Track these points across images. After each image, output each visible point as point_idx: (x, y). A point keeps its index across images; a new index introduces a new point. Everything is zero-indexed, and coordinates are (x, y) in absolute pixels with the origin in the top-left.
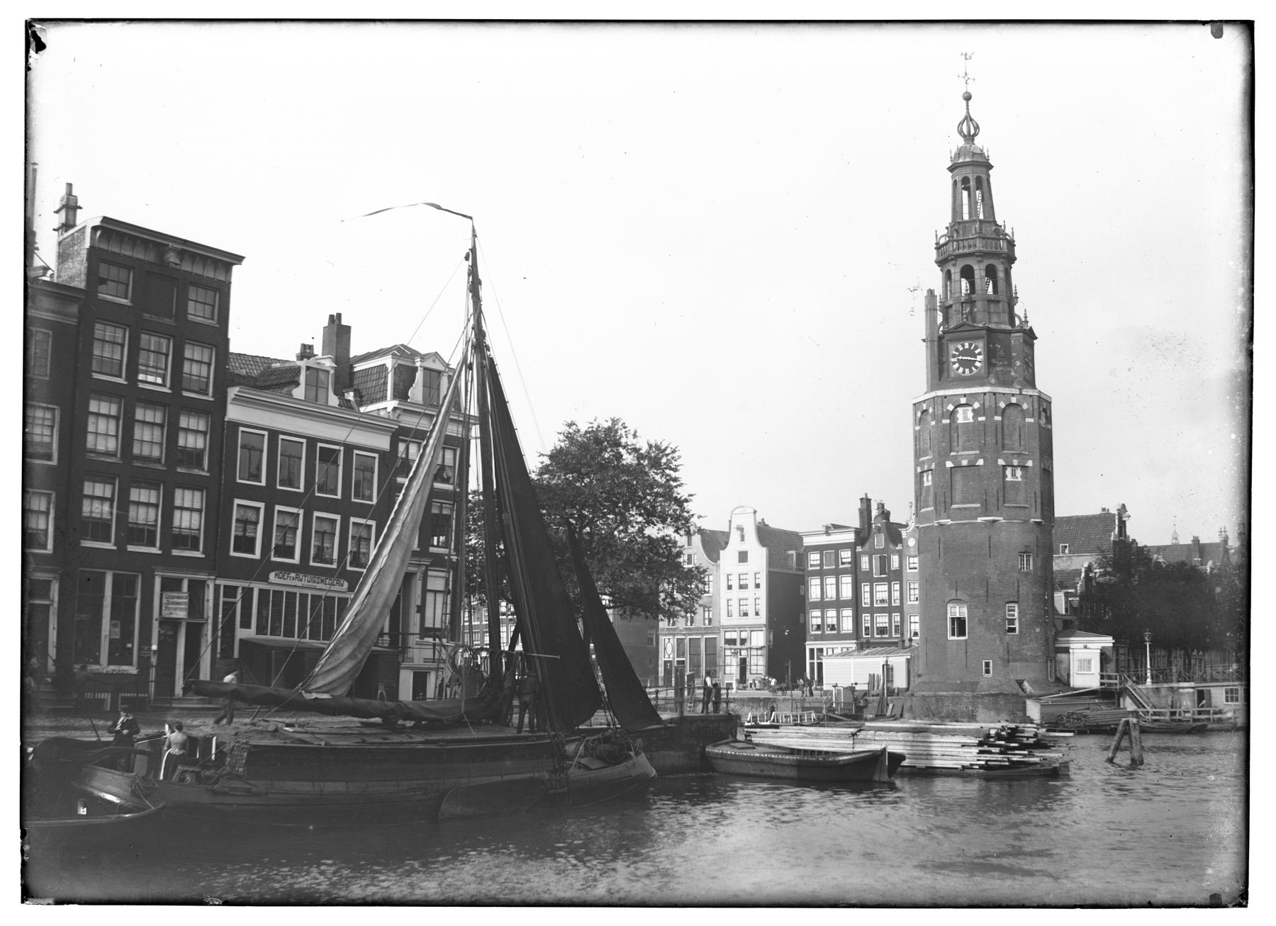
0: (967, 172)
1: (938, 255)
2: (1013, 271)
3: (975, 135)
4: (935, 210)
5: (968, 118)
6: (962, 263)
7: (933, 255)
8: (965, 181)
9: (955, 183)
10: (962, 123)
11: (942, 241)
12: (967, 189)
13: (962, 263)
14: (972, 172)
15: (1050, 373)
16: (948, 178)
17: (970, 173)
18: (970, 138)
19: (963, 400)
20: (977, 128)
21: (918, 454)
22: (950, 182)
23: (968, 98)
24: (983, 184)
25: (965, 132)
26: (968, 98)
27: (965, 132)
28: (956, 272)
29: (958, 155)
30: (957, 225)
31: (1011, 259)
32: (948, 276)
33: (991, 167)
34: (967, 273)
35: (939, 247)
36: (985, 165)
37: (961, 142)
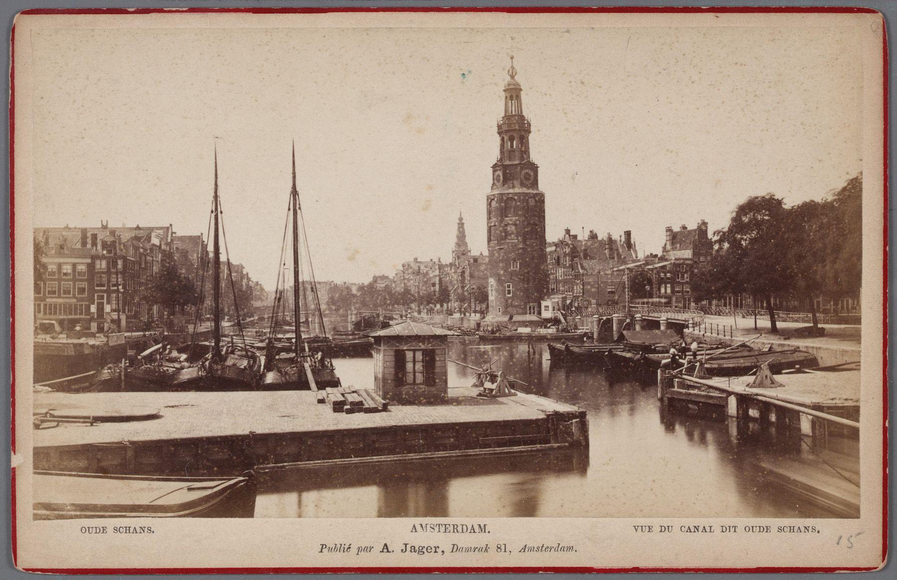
5: (513, 68)
7: (496, 129)
12: (512, 100)
14: (514, 93)
18: (512, 77)
21: (489, 218)
23: (512, 58)
24: (518, 97)
26: (512, 58)
28: (506, 138)
29: (509, 85)
30: (508, 117)
31: (530, 132)
32: (503, 139)
33: (521, 90)
34: (511, 139)
35: (499, 127)
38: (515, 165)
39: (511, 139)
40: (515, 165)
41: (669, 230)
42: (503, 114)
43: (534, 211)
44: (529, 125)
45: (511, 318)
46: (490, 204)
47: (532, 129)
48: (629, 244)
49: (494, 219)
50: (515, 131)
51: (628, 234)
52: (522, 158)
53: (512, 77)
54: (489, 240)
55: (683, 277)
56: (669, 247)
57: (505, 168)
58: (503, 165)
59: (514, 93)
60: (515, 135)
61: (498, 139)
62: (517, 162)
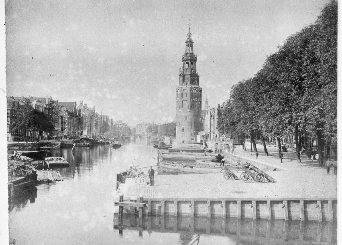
0: (189, 43)
1: (183, 59)
2: (196, 63)
3: (191, 36)
6: (186, 61)
7: (181, 59)
8: (188, 45)
10: (188, 33)
11: (183, 57)
12: (189, 46)
13: (186, 61)
16: (185, 44)
17: (189, 43)
18: (190, 36)
19: (185, 88)
20: (191, 34)
22: (185, 45)
25: (189, 35)
26: (190, 28)
27: (189, 35)
28: (185, 63)
30: (186, 54)
31: (196, 61)
32: (184, 63)
33: (193, 42)
34: (187, 63)
35: (183, 58)
44: (196, 58)
45: (183, 142)
47: (197, 59)
49: (178, 98)
52: (191, 72)
54: (177, 107)
57: (184, 76)
58: (183, 75)
59: (190, 43)
60: (189, 62)
61: (182, 63)
62: (189, 74)
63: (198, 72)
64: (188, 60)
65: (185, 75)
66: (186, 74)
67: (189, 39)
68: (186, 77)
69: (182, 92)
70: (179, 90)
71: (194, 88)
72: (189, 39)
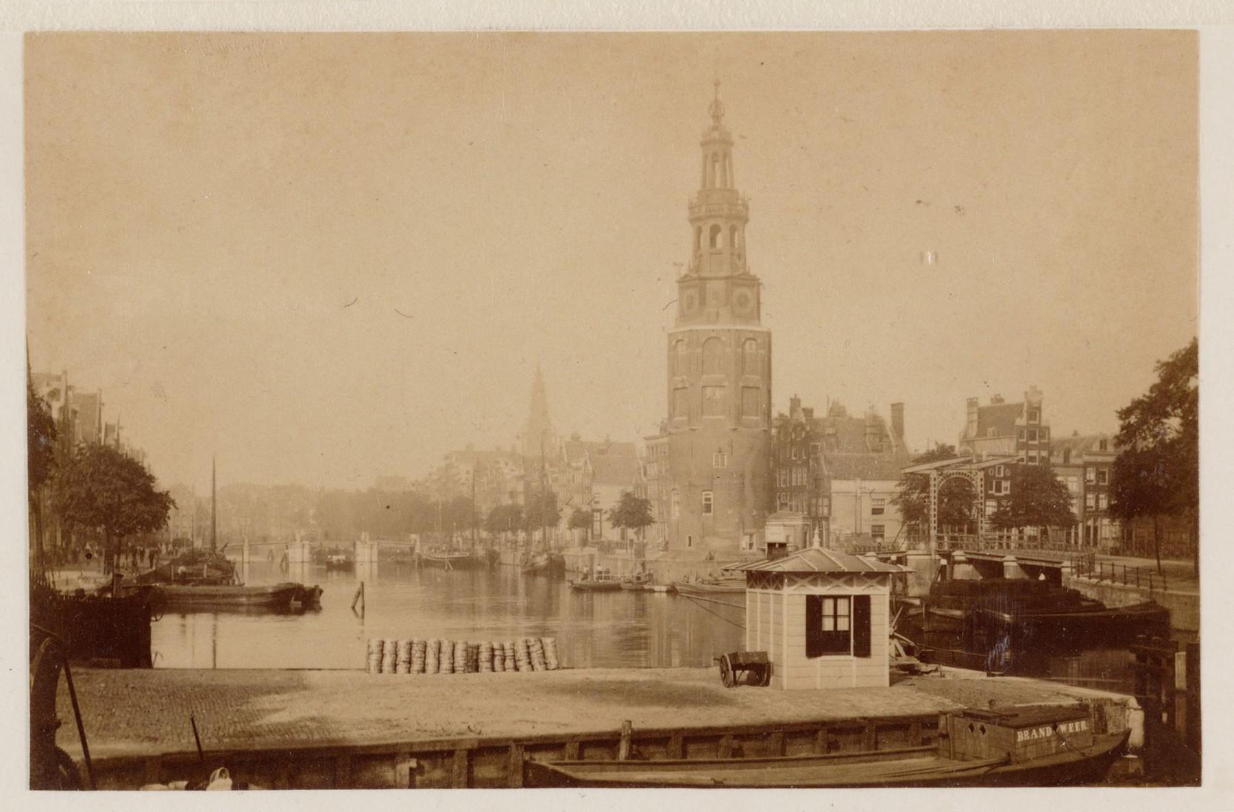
4: (687, 173)
5: (717, 104)
6: (712, 222)
7: (685, 214)
8: (715, 154)
9: (706, 157)
13: (712, 222)
14: (718, 149)
15: (773, 317)
18: (717, 117)
19: (713, 334)
21: (672, 372)
23: (717, 84)
26: (717, 84)
31: (746, 220)
35: (691, 208)
36: (727, 143)
37: (711, 122)
38: (720, 280)
39: (715, 230)
40: (720, 280)
41: (972, 403)
42: (698, 187)
43: (755, 366)
46: (672, 349)
47: (752, 215)
48: (899, 429)
50: (719, 218)
51: (897, 409)
53: (717, 117)
55: (999, 489)
56: (973, 432)
59: (718, 149)
60: (720, 222)
61: (688, 233)
63: (756, 264)
64: (720, 216)
65: (705, 279)
66: (712, 275)
67: (715, 129)
68: (712, 286)
69: (699, 350)
70: (686, 340)
71: (751, 335)
72: (715, 129)
